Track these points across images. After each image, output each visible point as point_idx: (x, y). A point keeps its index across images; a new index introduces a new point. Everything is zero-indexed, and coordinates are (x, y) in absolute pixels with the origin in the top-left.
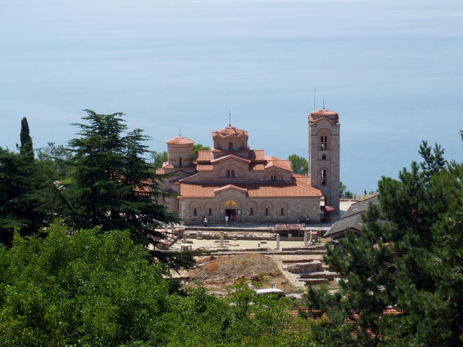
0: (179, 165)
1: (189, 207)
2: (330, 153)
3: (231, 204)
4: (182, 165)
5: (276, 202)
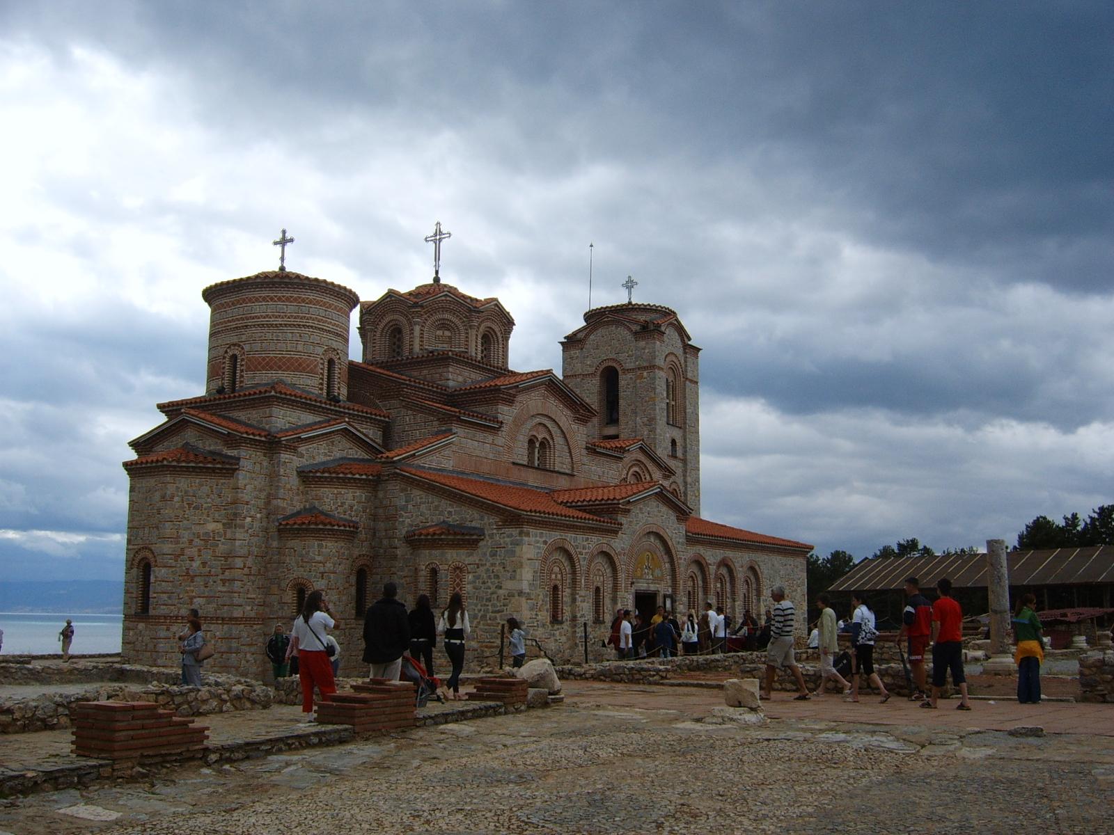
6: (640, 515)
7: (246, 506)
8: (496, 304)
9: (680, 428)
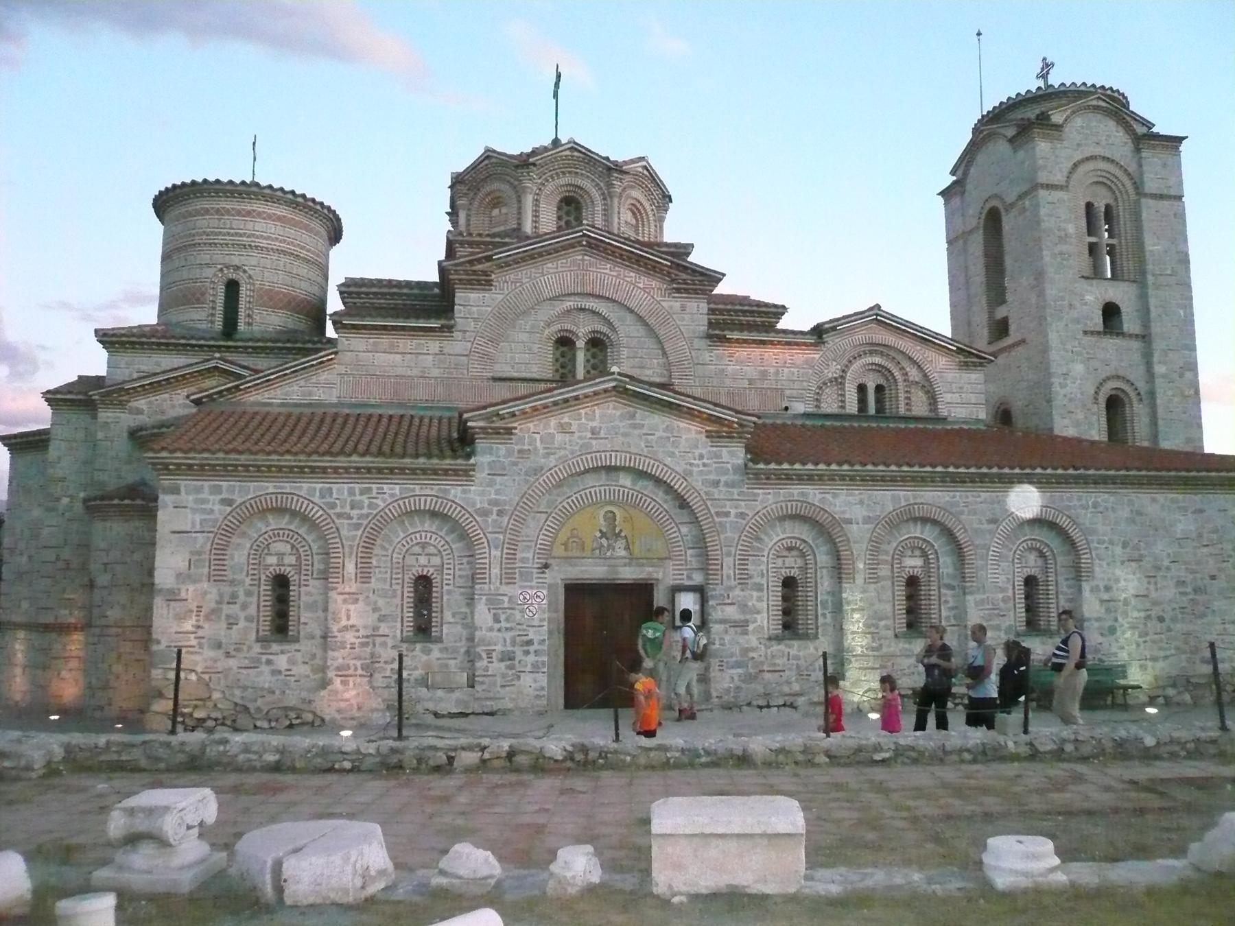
0: (218, 325)
1: (220, 550)
2: (1143, 297)
3: (611, 533)
4: (242, 327)
5: (994, 521)
6: (559, 438)
7: (60, 484)
8: (572, 148)
9: (1134, 281)
